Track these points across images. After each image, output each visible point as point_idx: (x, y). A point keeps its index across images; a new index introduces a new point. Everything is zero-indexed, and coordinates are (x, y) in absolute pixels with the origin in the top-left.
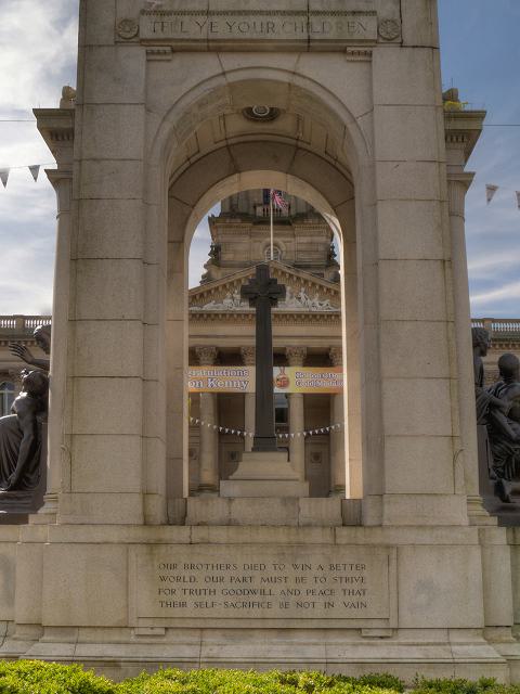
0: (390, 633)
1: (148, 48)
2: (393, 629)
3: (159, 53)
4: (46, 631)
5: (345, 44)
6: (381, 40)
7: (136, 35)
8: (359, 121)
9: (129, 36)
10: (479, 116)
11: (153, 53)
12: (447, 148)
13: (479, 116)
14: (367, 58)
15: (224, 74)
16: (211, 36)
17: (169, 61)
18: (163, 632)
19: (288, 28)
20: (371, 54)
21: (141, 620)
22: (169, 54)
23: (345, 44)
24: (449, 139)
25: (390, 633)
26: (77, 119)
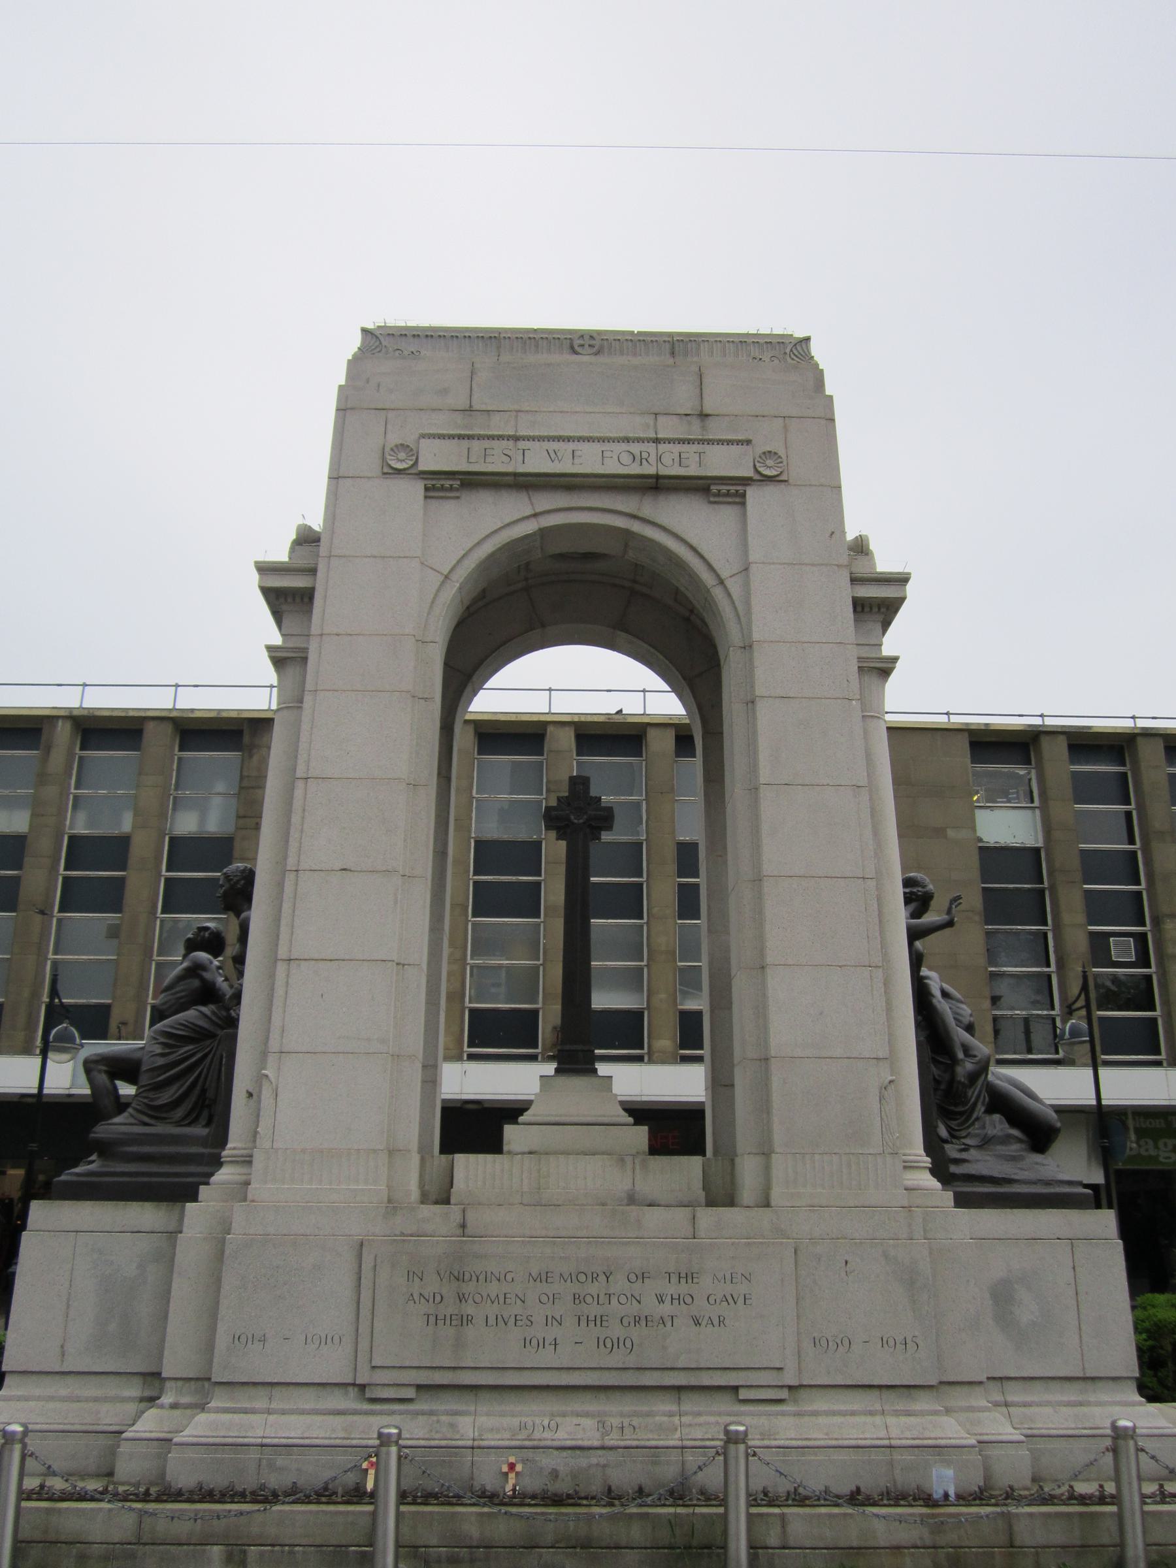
0: (784, 1394)
1: (426, 482)
2: (790, 1388)
3: (442, 488)
4: (217, 1389)
5: (709, 482)
6: (757, 477)
7: (413, 466)
8: (728, 583)
9: (400, 466)
10: (902, 580)
11: (434, 488)
12: (856, 620)
13: (902, 580)
14: (737, 500)
15: (535, 515)
16: (521, 469)
17: (458, 498)
18: (410, 1393)
19: (626, 459)
20: (744, 495)
21: (378, 1372)
22: (457, 490)
23: (709, 482)
24: (859, 609)
25: (784, 1394)
26: (320, 574)
